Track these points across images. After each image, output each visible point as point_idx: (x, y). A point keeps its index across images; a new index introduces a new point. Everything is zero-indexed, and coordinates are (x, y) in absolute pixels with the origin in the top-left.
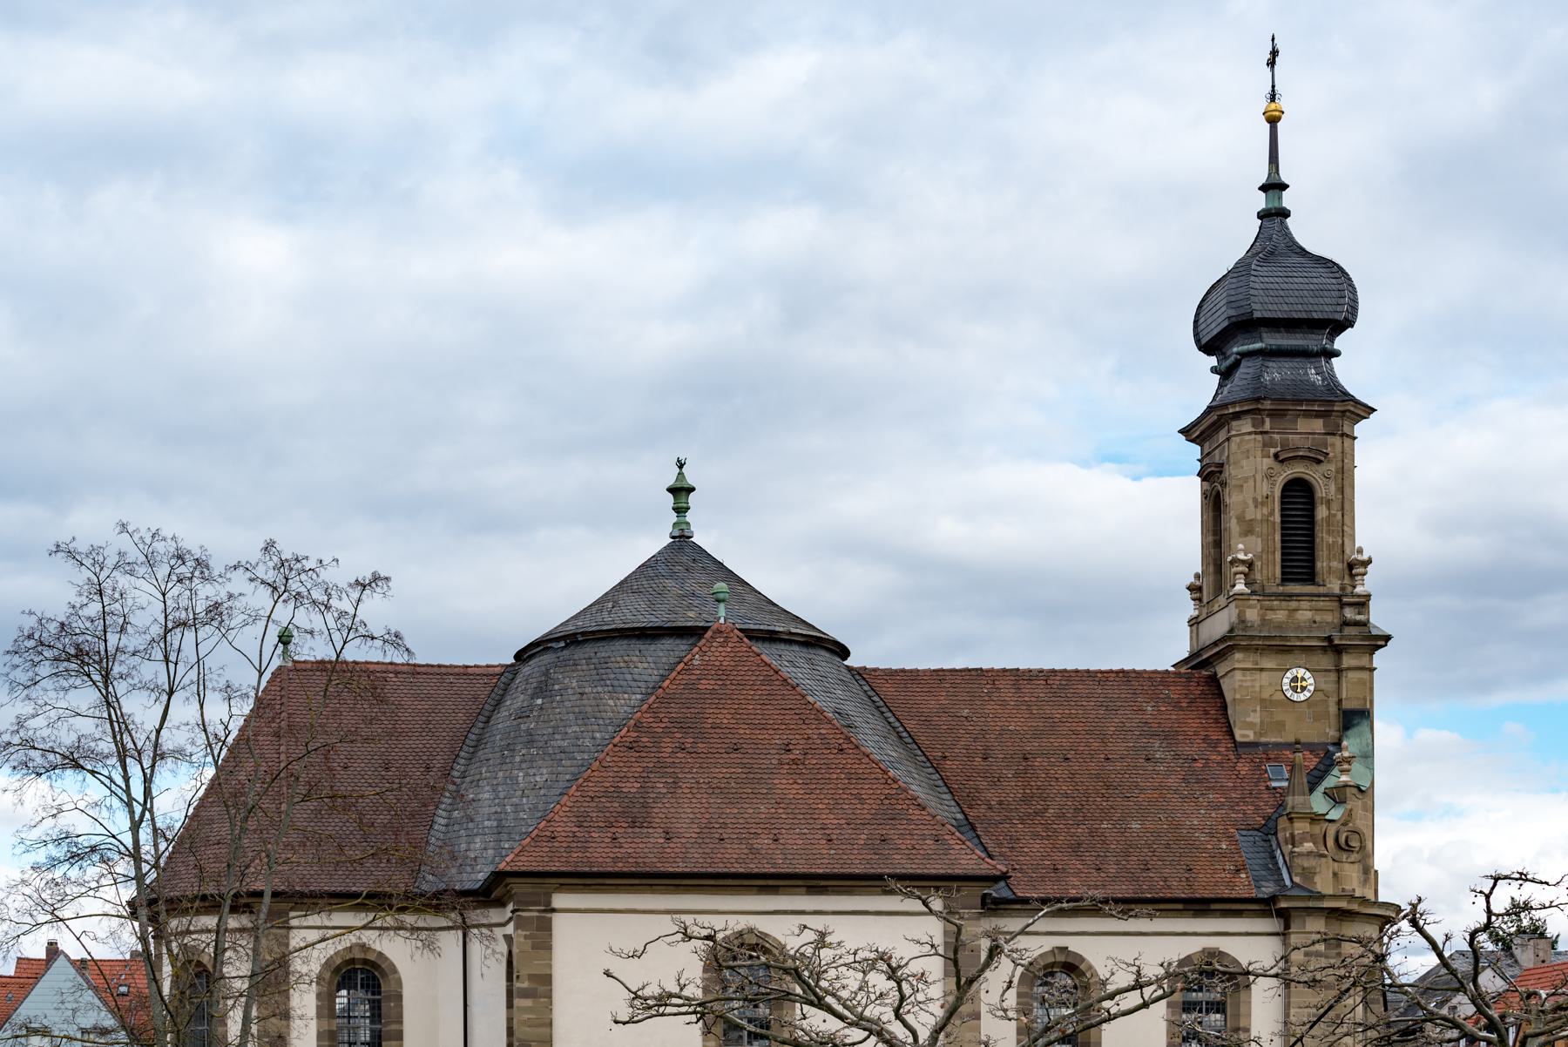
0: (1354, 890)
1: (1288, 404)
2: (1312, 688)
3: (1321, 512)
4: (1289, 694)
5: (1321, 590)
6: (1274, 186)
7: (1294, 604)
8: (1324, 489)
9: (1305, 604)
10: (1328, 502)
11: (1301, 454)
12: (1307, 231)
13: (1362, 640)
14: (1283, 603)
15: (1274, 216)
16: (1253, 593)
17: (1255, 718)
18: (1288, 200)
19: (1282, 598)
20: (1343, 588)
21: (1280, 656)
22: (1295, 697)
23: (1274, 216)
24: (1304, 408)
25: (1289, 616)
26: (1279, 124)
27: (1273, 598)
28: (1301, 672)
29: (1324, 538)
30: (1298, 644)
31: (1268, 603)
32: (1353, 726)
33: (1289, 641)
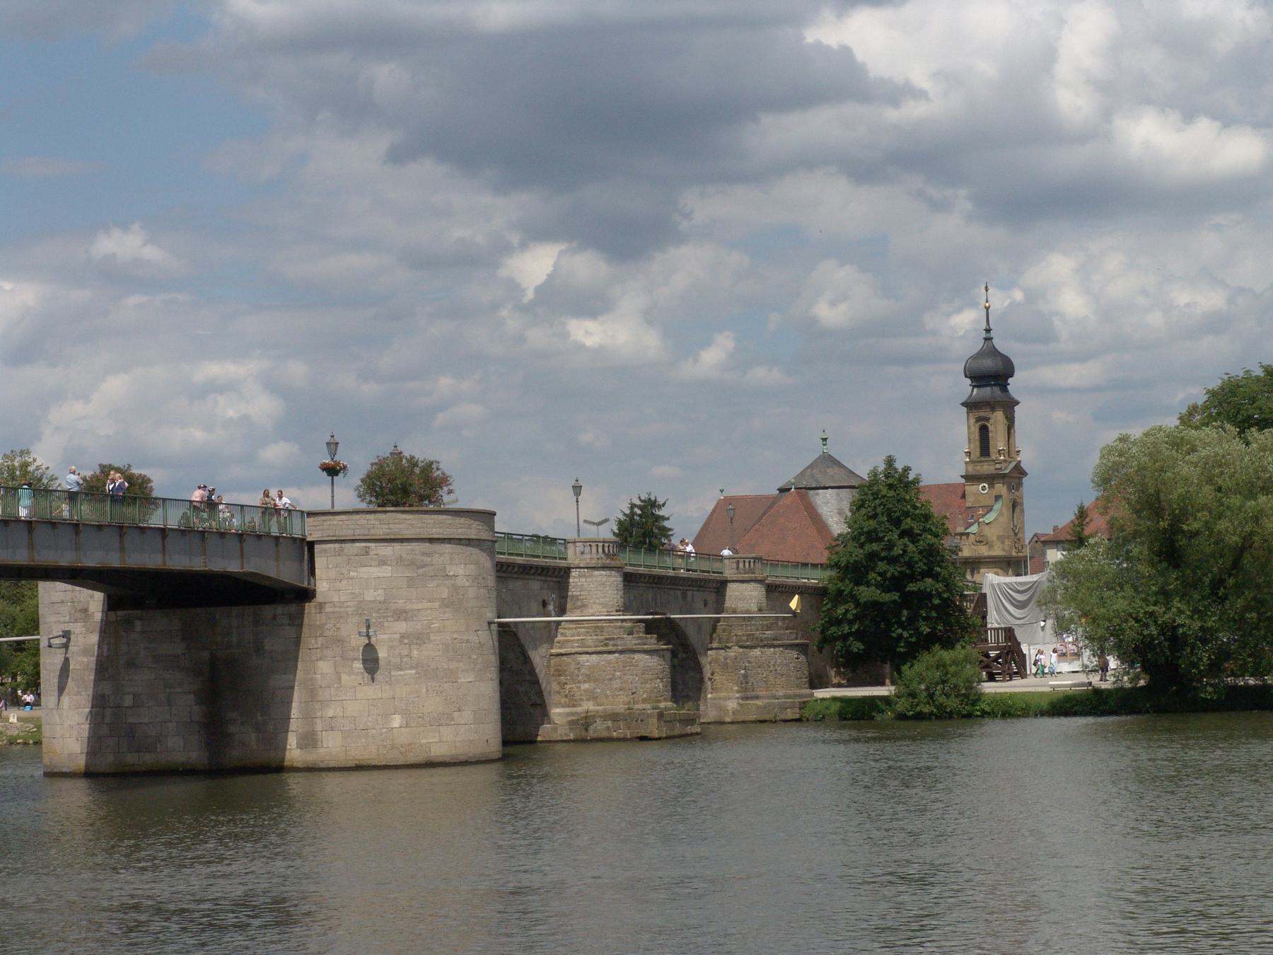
3: (990, 435)
4: (982, 491)
5: (990, 459)
6: (988, 331)
8: (991, 428)
9: (985, 464)
10: (992, 432)
12: (999, 344)
15: (988, 339)
16: (970, 461)
18: (992, 334)
22: (983, 492)
23: (988, 339)
26: (989, 310)
28: (986, 485)
29: (991, 443)
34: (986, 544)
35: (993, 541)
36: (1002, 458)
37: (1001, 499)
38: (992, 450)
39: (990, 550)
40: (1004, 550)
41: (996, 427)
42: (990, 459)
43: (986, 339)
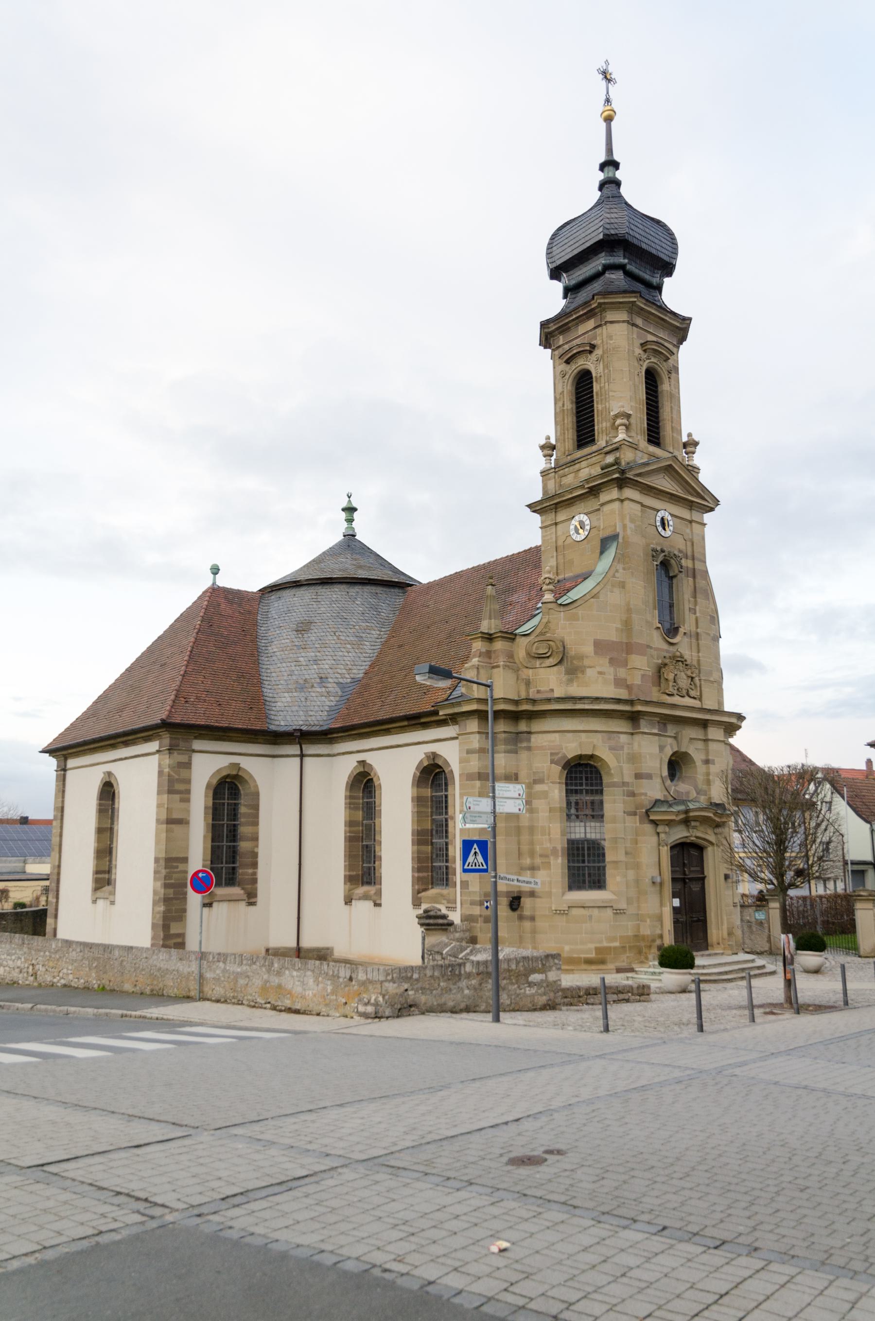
0: (552, 690)
1: (564, 319)
2: (588, 528)
3: (596, 387)
7: (577, 467)
9: (584, 464)
11: (575, 352)
13: (602, 478)
14: (571, 468)
17: (553, 562)
19: (569, 465)
20: (607, 442)
21: (568, 509)
24: (574, 317)
25: (575, 477)
26: (612, 123)
27: (564, 467)
30: (570, 496)
31: (562, 471)
32: (606, 550)
33: (564, 496)
34: (560, 662)
35: (581, 657)
36: (622, 435)
37: (615, 545)
38: (601, 425)
39: (570, 681)
40: (619, 682)
41: (606, 367)
42: (594, 448)
43: (602, 186)
